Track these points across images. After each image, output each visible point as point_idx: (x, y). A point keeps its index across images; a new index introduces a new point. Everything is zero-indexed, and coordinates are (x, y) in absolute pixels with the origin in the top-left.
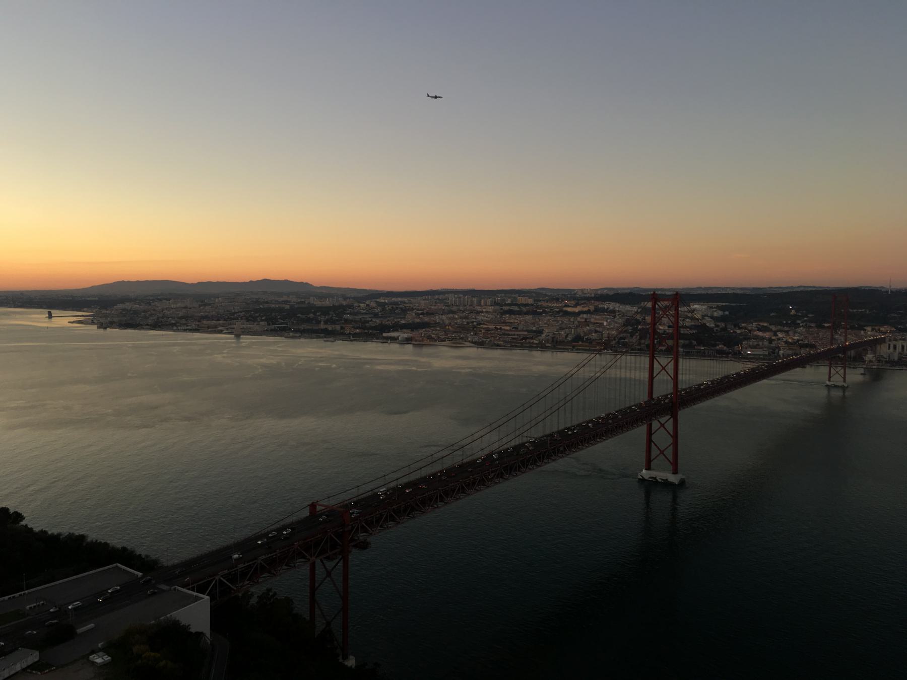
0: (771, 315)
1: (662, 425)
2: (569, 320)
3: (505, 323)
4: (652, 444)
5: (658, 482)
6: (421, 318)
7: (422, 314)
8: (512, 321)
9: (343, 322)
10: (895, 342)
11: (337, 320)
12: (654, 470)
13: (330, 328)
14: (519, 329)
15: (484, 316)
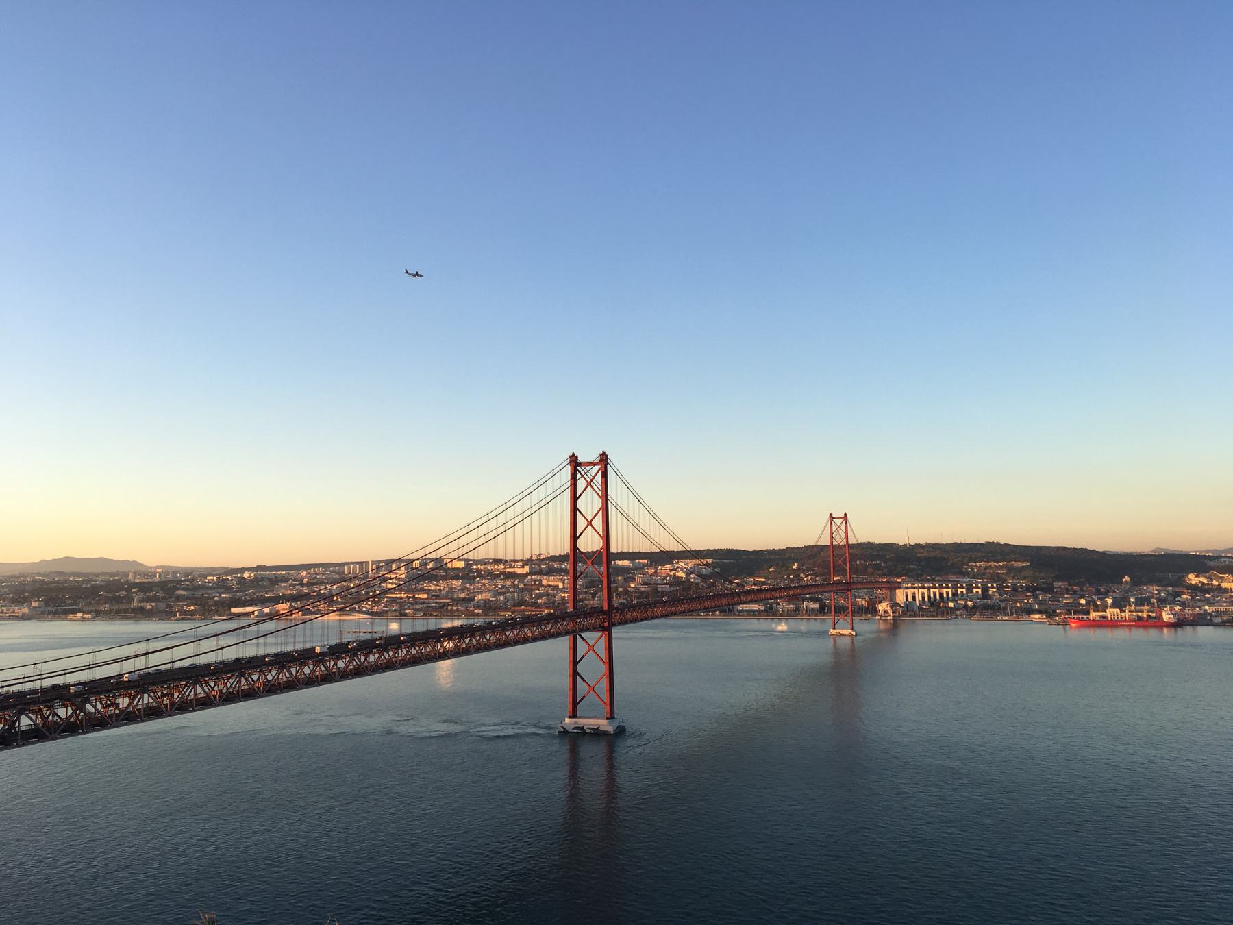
0: (770, 570)
1: (592, 648)
2: (513, 583)
3: (422, 590)
4: (578, 677)
5: (584, 733)
6: (297, 590)
7: (302, 584)
8: (432, 587)
9: (173, 599)
10: (913, 590)
11: (163, 598)
12: (580, 717)
13: (148, 606)
14: (442, 597)
15: (392, 583)
